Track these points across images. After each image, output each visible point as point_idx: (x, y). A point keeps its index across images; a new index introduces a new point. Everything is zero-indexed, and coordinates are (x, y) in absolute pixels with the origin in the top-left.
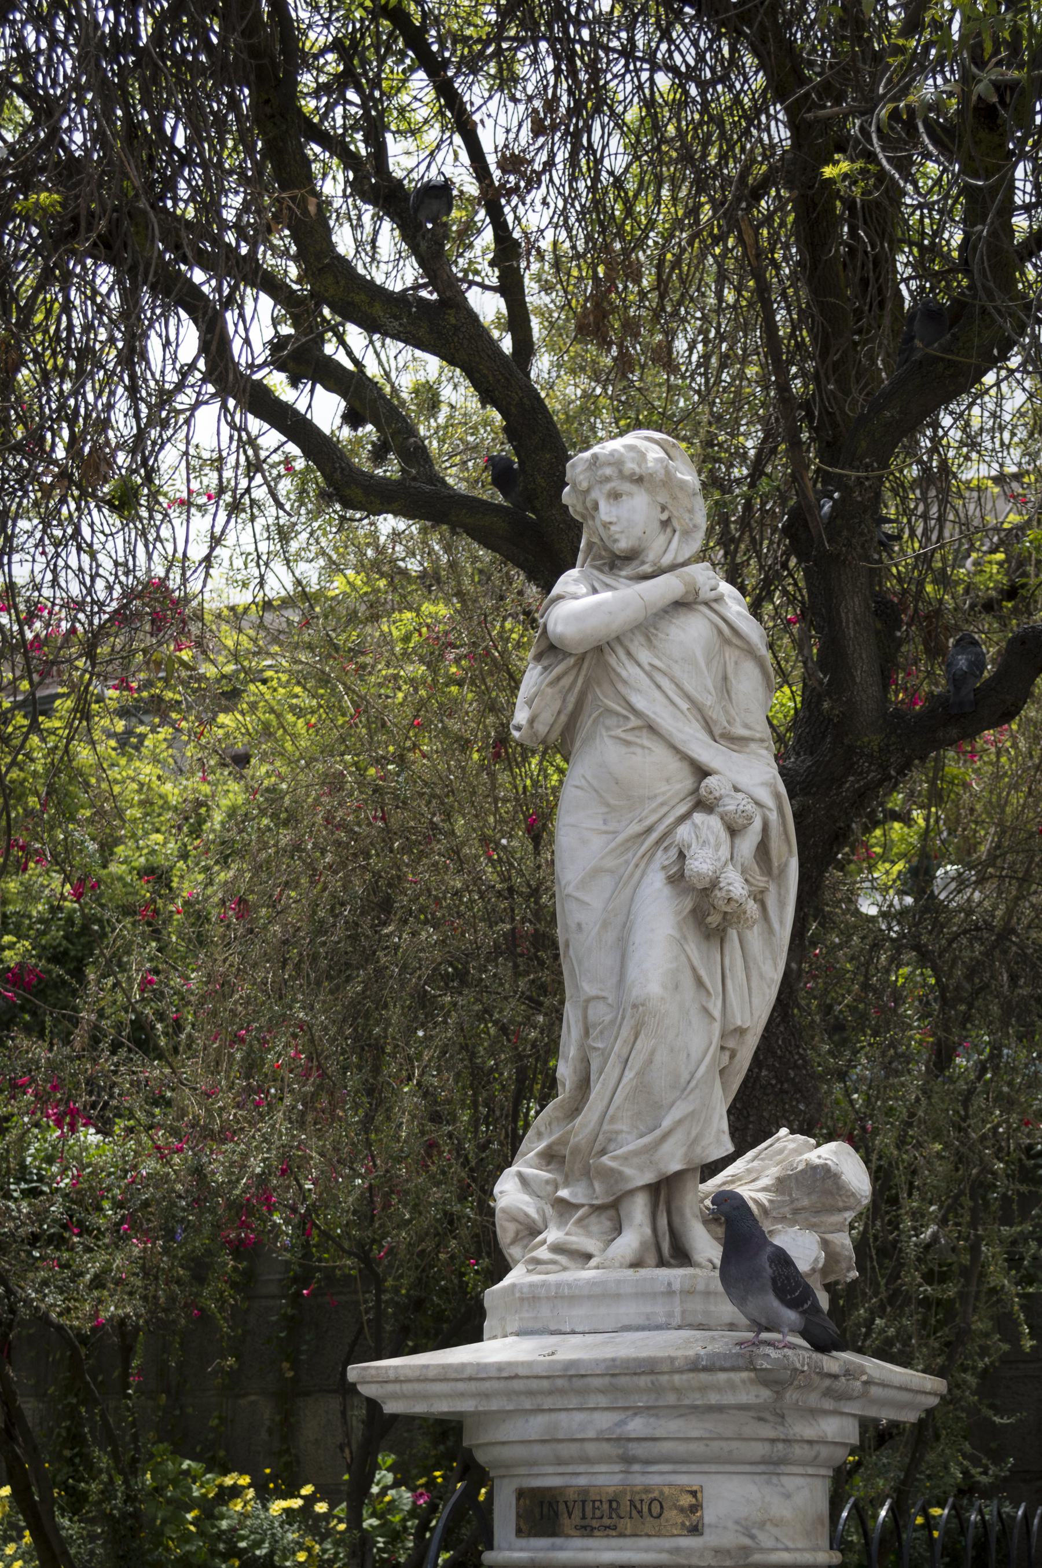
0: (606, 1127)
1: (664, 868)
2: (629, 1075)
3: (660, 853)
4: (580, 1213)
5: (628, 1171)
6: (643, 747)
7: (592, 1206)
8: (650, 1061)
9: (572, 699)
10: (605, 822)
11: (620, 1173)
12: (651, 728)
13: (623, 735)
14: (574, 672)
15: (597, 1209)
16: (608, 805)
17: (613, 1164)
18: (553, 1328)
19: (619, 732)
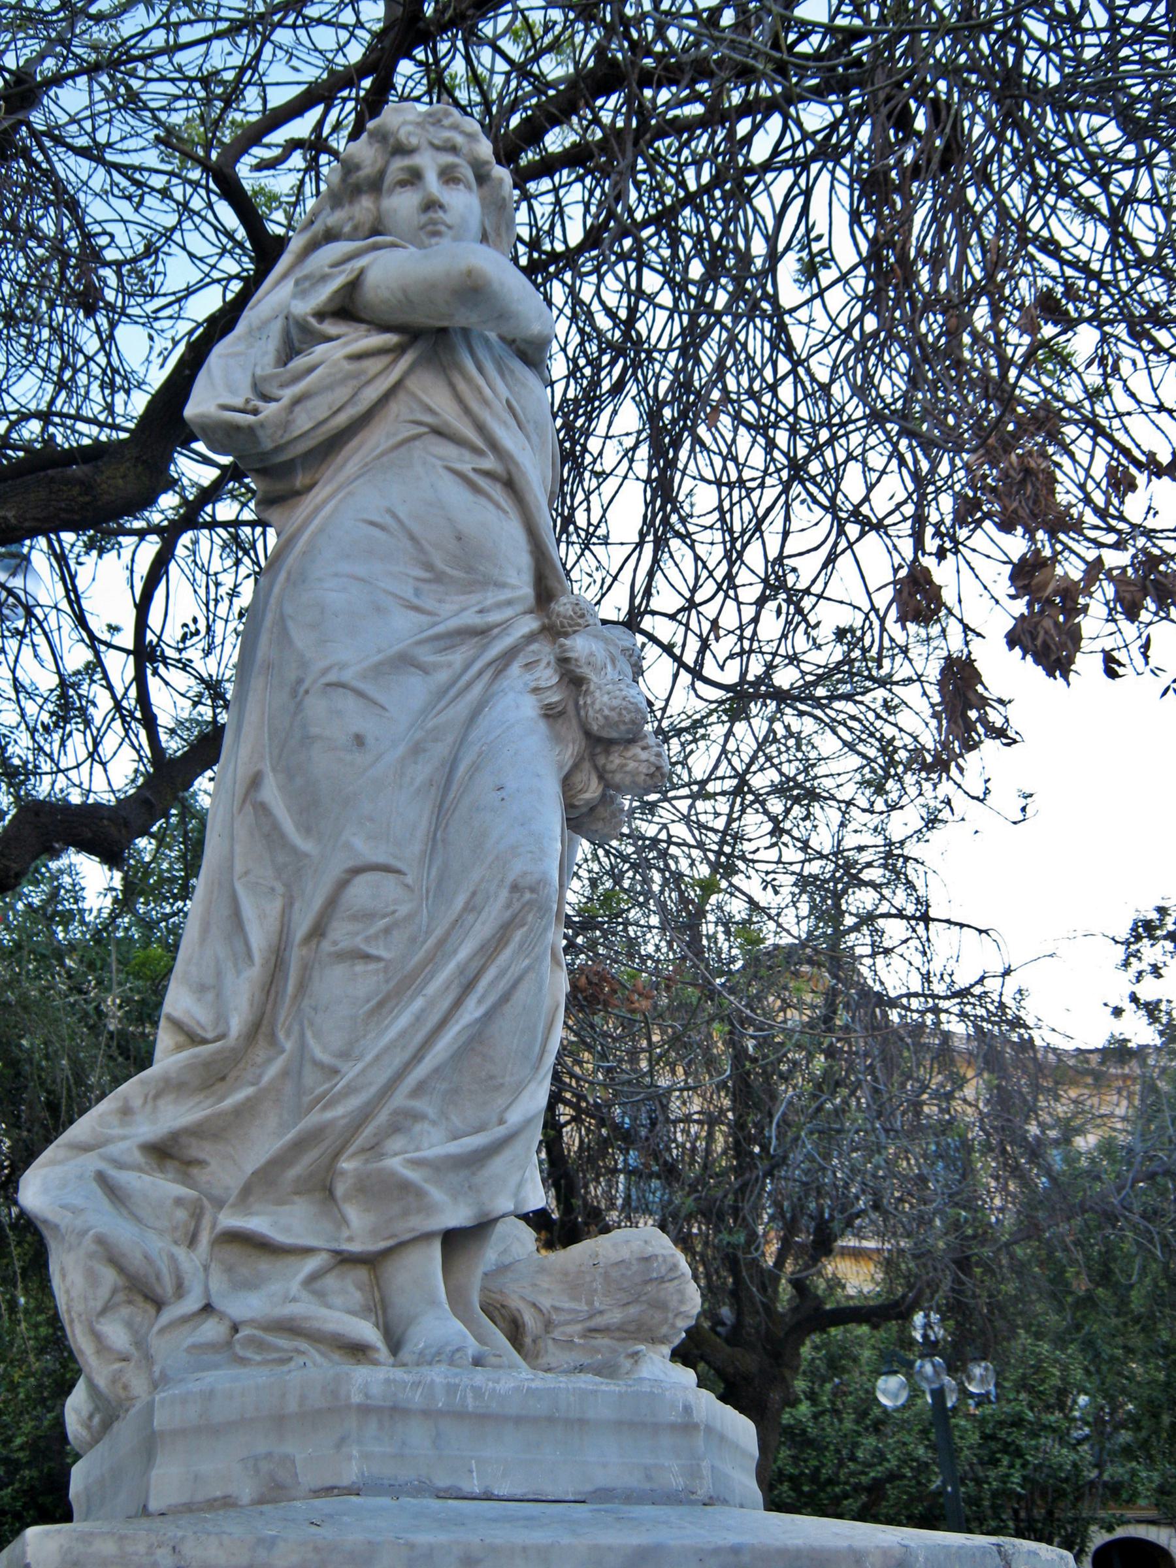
0: (399, 1099)
1: (536, 690)
2: (472, 1011)
3: (515, 669)
4: (311, 1264)
5: (436, 1194)
6: (498, 506)
7: (337, 1253)
8: (506, 998)
9: (371, 394)
10: (417, 593)
11: (420, 1193)
12: (511, 484)
13: (472, 475)
14: (385, 360)
15: (344, 1260)
16: (429, 566)
17: (413, 1175)
18: (442, 1481)
19: (466, 468)
